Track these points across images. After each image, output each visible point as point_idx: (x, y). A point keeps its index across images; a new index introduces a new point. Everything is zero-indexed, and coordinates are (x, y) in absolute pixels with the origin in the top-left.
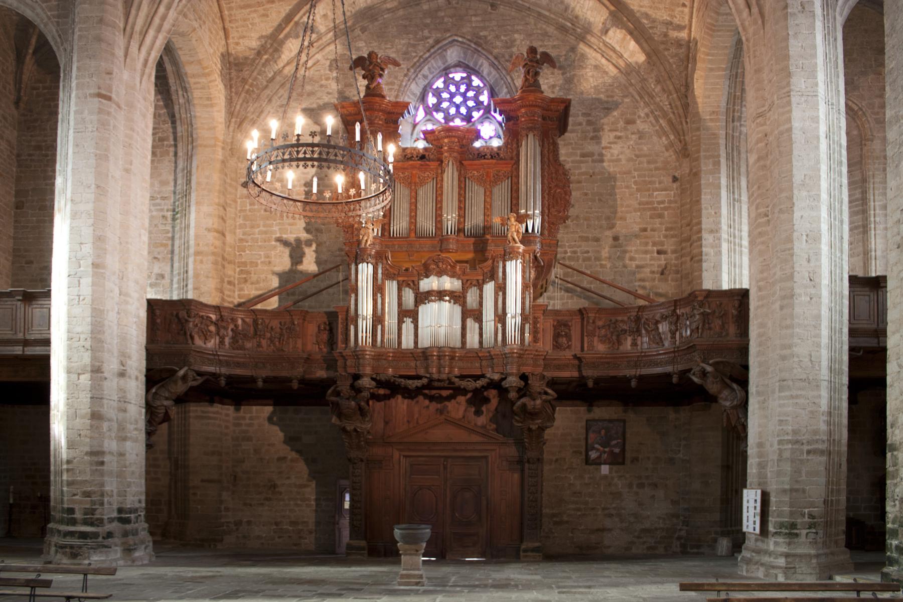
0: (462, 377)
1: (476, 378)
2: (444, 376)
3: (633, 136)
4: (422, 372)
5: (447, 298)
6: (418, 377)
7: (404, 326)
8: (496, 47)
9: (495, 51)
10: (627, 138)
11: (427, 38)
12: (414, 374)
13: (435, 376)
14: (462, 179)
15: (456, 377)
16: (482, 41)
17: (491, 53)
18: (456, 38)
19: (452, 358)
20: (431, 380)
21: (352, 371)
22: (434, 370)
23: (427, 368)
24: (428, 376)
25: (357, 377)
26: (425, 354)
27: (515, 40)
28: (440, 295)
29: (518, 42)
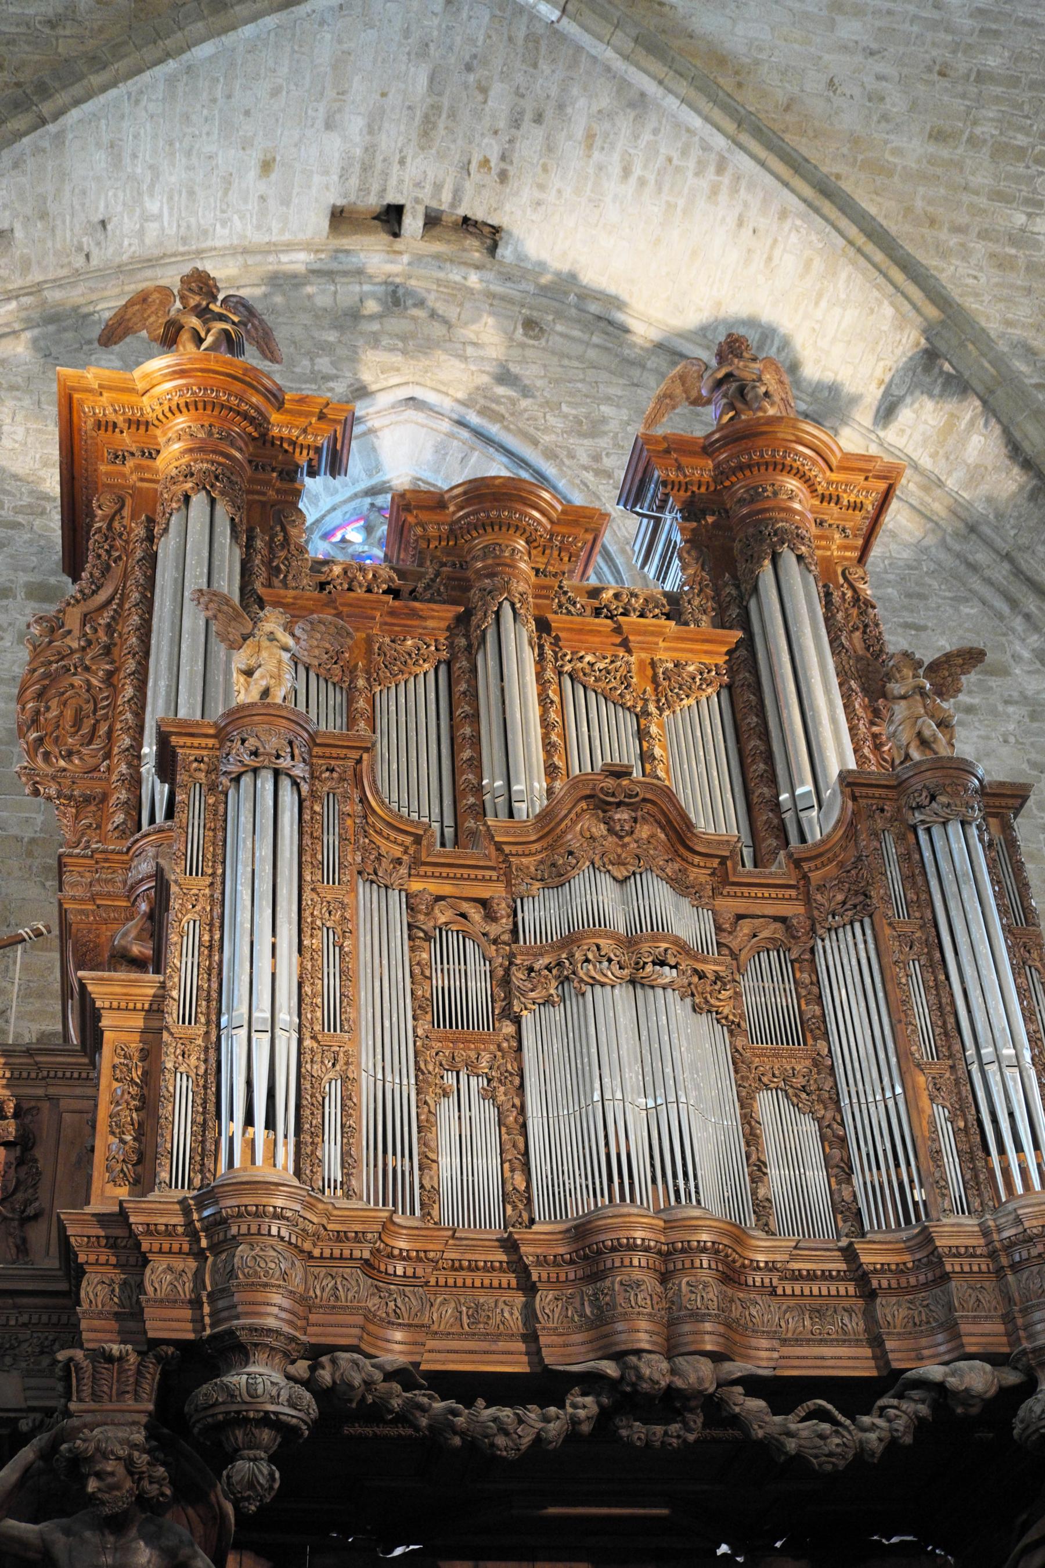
0: (783, 1392)
1: (853, 1395)
2: (700, 1374)
3: (1011, 709)
4: (567, 1351)
5: (668, 974)
6: (544, 1386)
7: (446, 1110)
8: (546, 430)
9: (546, 439)
10: (993, 712)
11: (327, 378)
12: (519, 1366)
13: (655, 1369)
14: (549, 674)
15: (753, 1385)
16: (502, 409)
17: (535, 443)
18: (419, 393)
19: (732, 1275)
20: (626, 1398)
21: (169, 1324)
22: (643, 1334)
23: (601, 1321)
24: (610, 1369)
25: (226, 1349)
26: (590, 1251)
27: (604, 420)
28: (641, 960)
29: (613, 426)
